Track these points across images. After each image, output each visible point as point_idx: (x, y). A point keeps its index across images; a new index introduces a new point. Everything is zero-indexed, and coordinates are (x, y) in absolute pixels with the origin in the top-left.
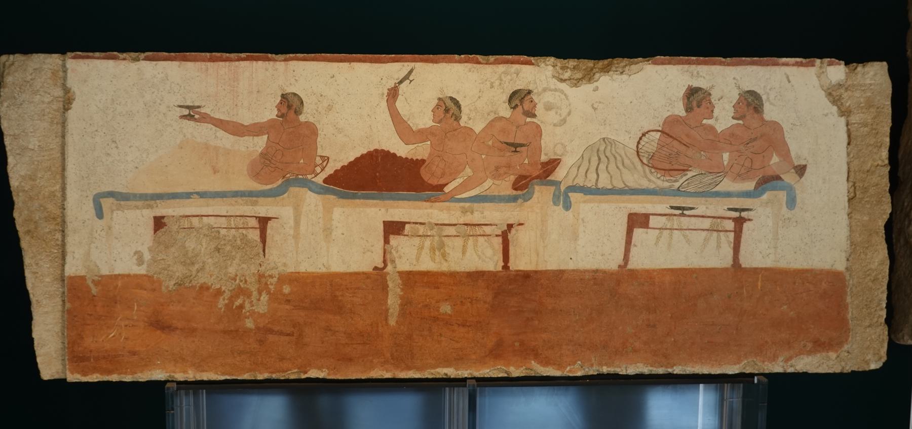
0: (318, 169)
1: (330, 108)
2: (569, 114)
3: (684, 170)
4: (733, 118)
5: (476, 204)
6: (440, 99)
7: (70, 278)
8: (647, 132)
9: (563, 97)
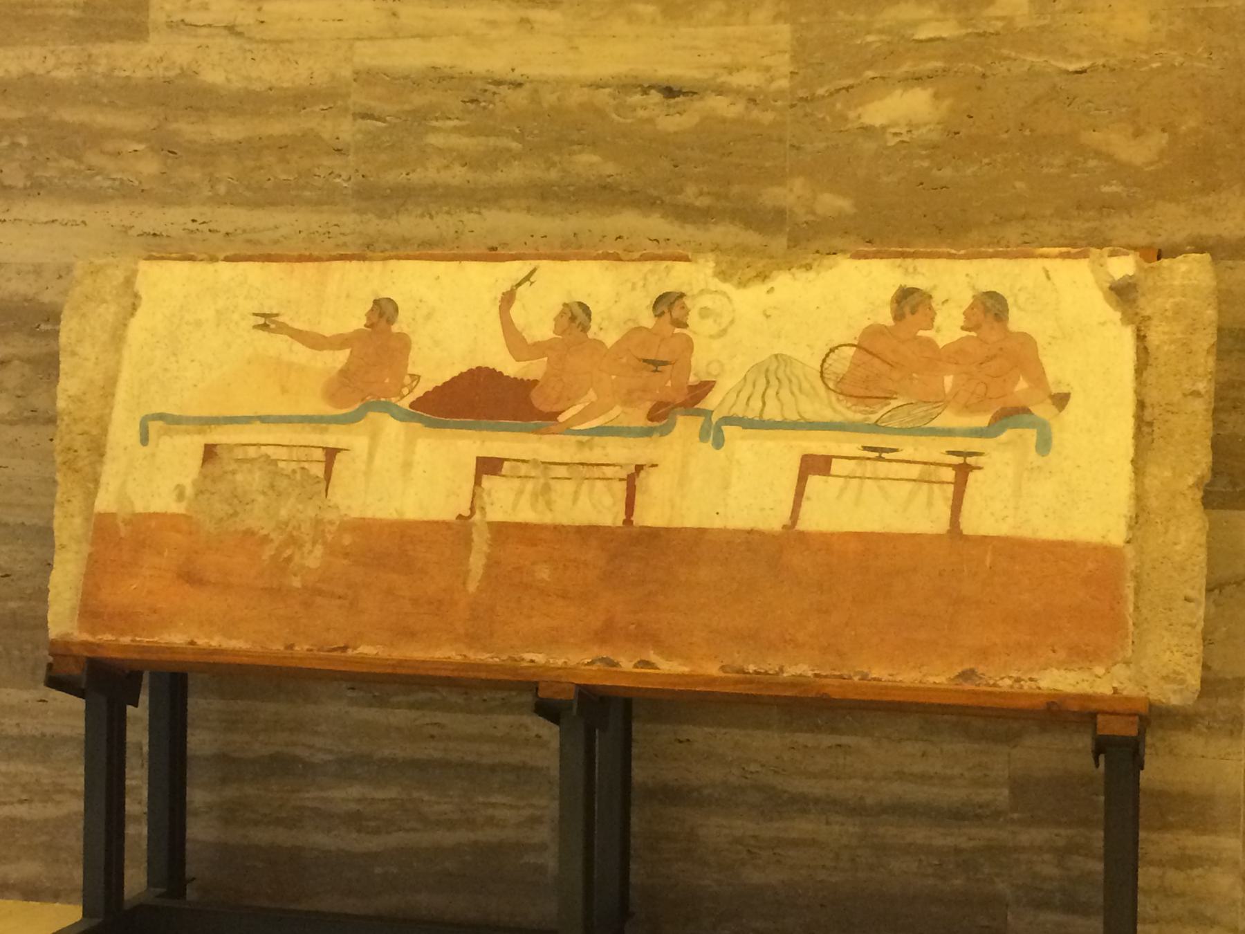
0: (405, 391)
1: (429, 316)
2: (732, 322)
3: (886, 398)
4: (963, 328)
5: (597, 439)
6: (565, 305)
7: (102, 516)
8: (837, 348)
9: (725, 300)
